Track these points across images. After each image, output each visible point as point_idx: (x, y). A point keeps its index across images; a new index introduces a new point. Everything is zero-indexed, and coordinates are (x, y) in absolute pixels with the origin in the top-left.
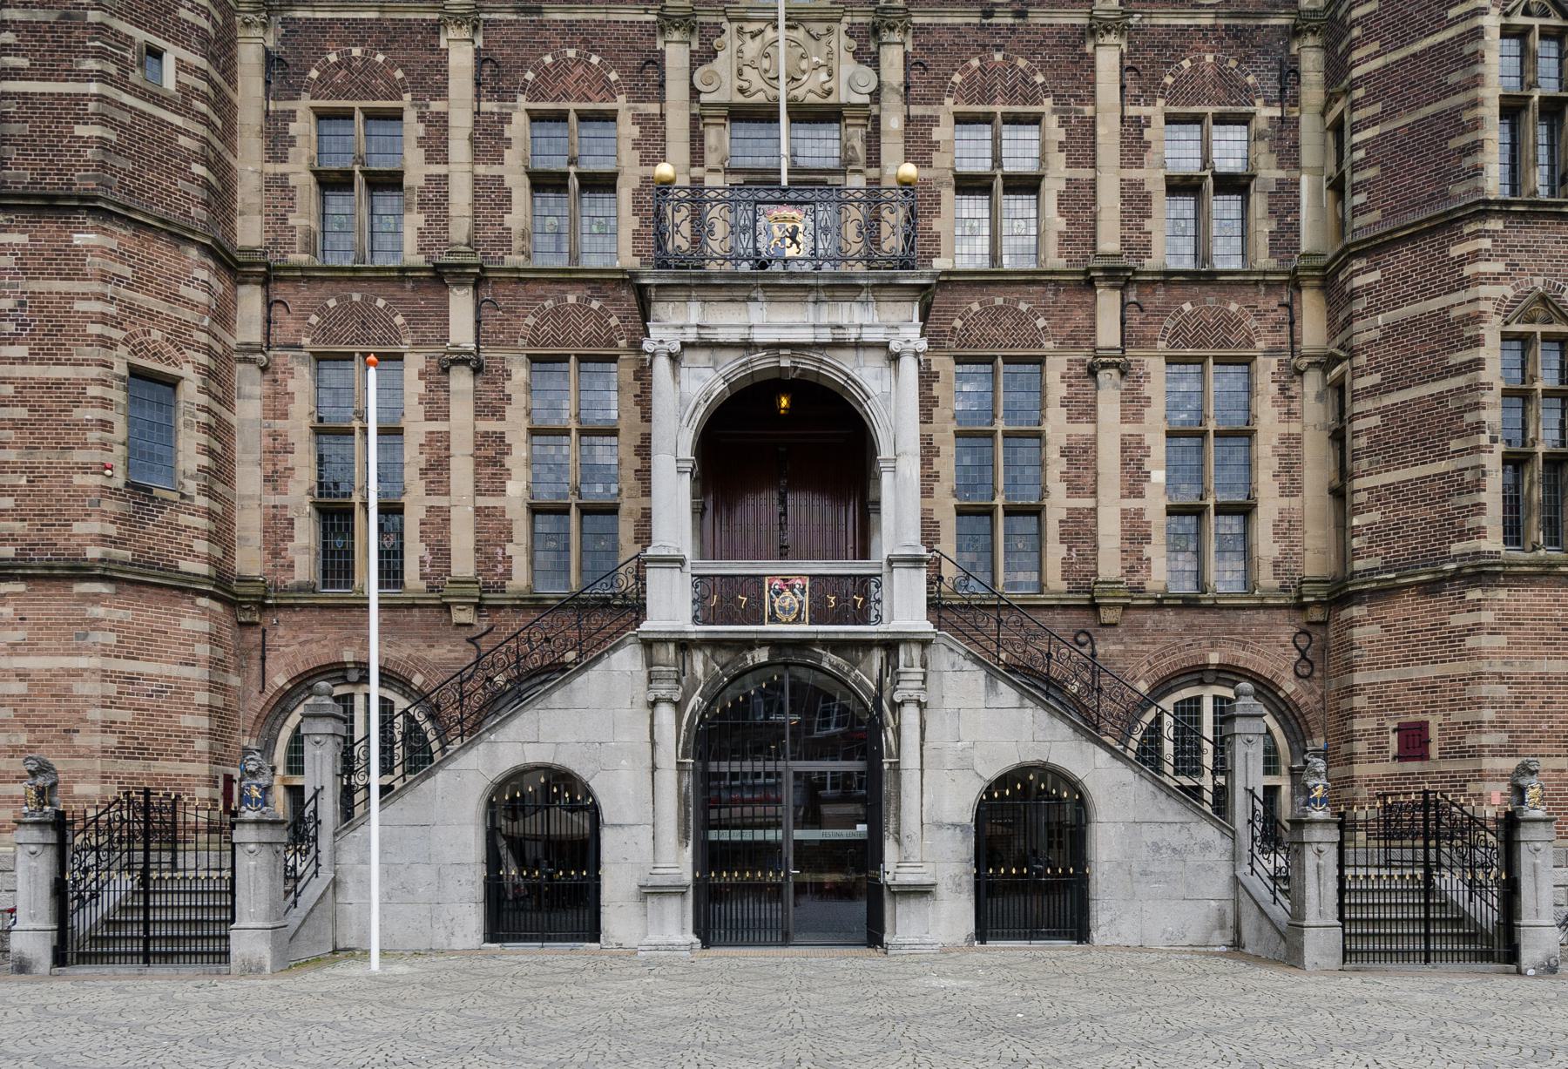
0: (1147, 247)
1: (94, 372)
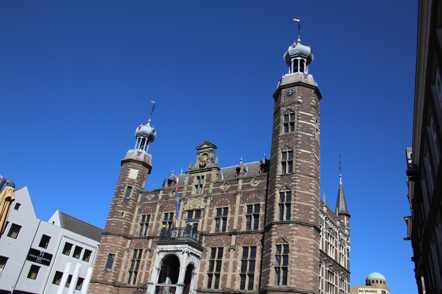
0: (241, 228)
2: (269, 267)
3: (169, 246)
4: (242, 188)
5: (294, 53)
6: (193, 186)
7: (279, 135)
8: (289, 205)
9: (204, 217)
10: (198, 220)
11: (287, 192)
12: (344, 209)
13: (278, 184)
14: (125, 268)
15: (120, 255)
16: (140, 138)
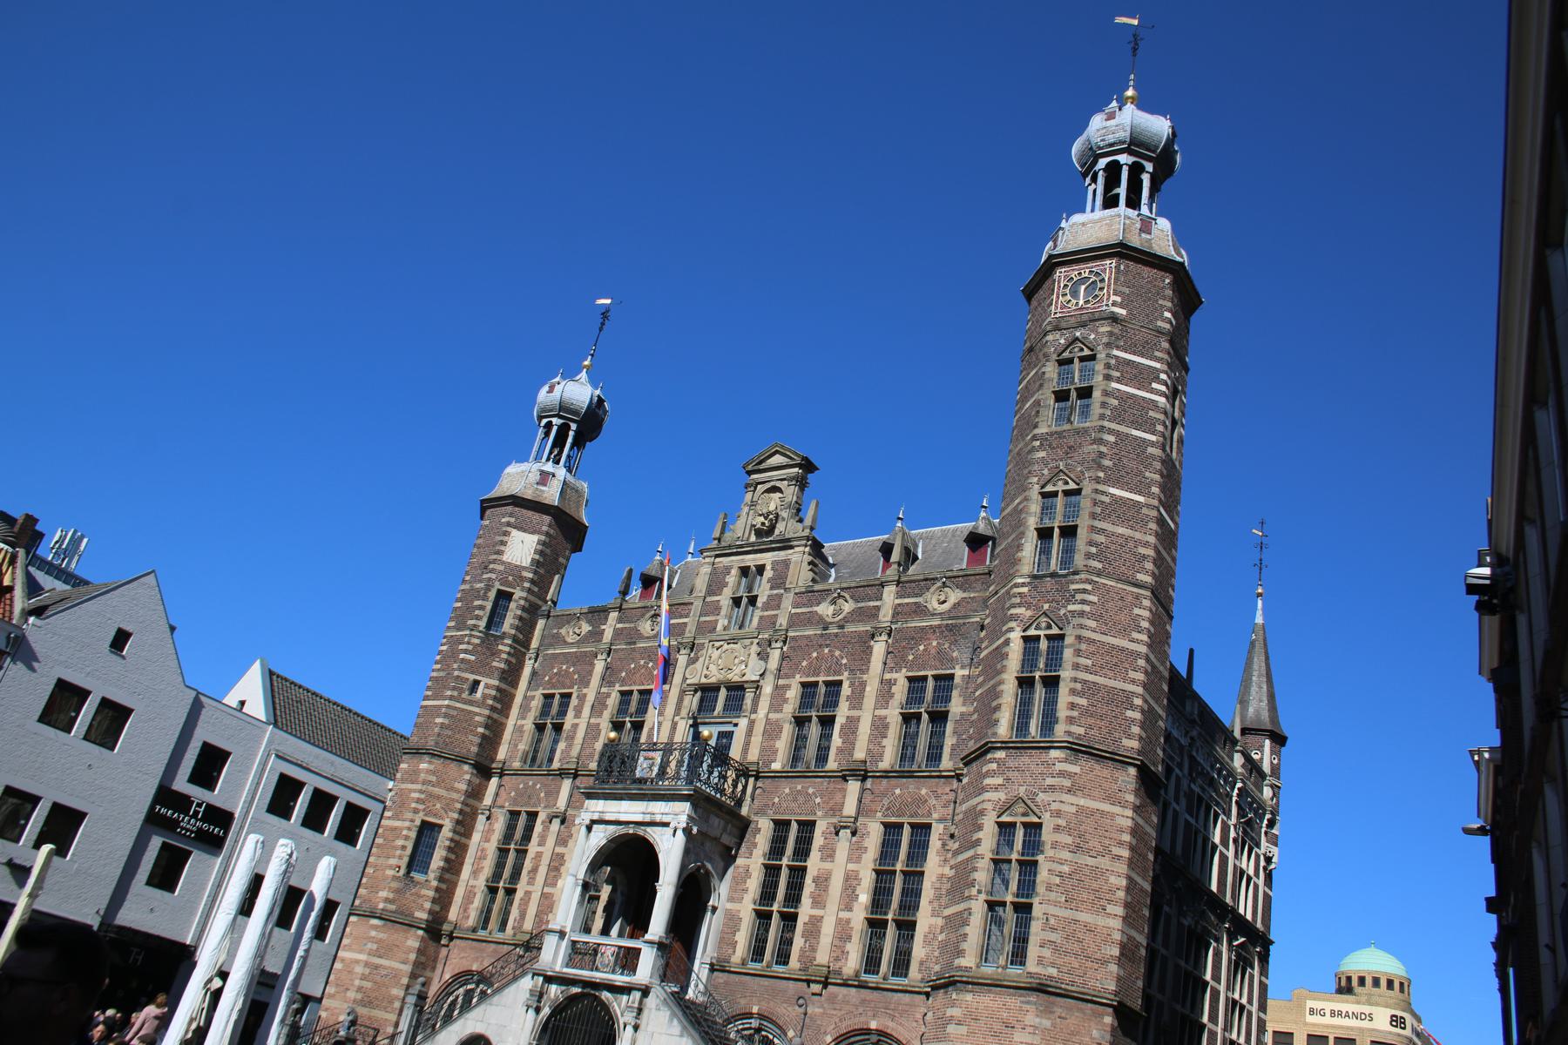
2: (970, 898)
3: (625, 805)
4: (896, 614)
5: (1111, 139)
6: (725, 599)
7: (1036, 431)
8: (1052, 683)
9: (754, 710)
11: (1048, 637)
12: (1265, 715)
13: (1020, 605)
15: (459, 828)
16: (549, 426)
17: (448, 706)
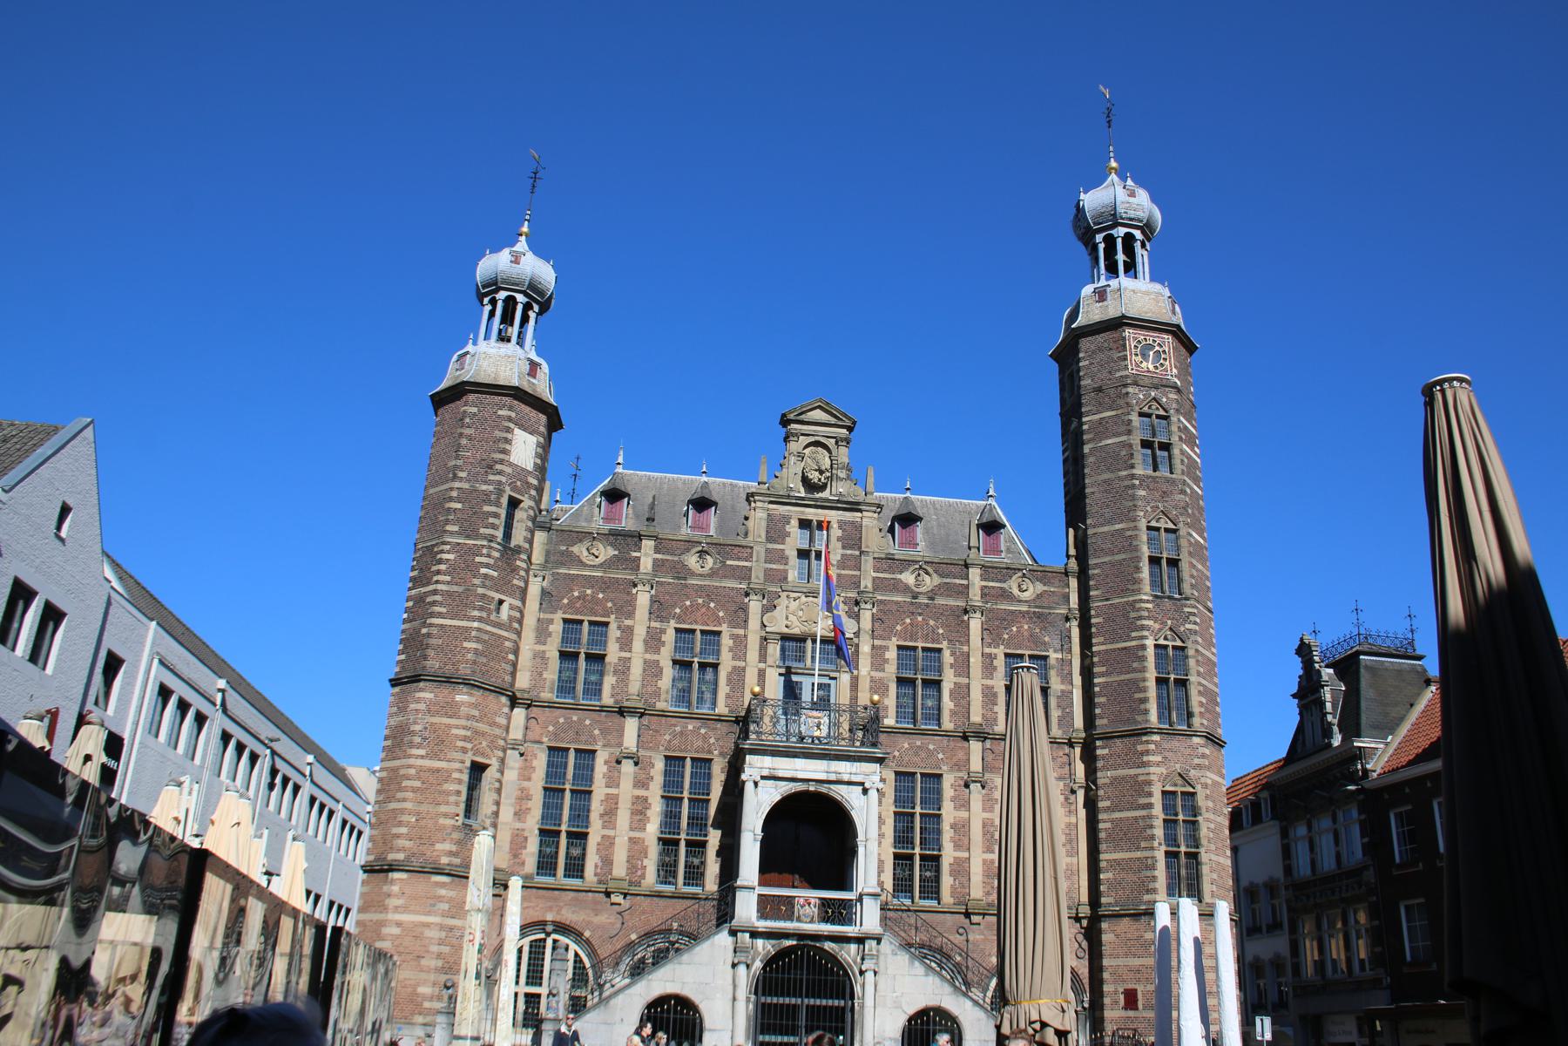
0: (995, 720)
1: (458, 765)
2: (1152, 848)
4: (983, 595)
5: (1132, 214)
10: (833, 674)
11: (1174, 647)
13: (1148, 618)
14: (519, 814)
16: (510, 303)
17: (479, 630)
